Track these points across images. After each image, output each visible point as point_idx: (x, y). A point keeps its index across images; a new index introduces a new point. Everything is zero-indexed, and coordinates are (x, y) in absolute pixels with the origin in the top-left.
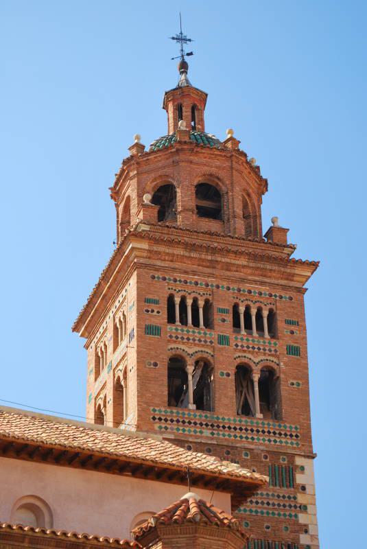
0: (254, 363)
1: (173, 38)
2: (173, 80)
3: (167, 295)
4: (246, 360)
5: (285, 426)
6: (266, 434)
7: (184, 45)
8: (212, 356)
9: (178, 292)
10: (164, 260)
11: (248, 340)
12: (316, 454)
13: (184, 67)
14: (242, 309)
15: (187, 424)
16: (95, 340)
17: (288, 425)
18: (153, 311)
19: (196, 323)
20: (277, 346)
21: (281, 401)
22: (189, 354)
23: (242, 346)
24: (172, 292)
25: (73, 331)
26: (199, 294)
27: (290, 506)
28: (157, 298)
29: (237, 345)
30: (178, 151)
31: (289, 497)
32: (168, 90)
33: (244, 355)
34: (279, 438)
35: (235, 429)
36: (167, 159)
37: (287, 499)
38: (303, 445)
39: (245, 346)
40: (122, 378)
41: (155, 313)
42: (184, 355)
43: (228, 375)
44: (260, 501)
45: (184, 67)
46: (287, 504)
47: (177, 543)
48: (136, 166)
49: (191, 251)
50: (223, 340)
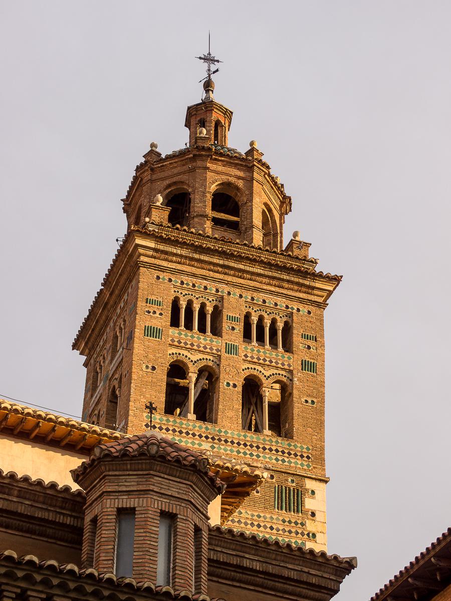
0: (265, 376)
1: (200, 58)
2: (197, 96)
3: (172, 298)
4: (255, 373)
5: (295, 446)
6: (274, 452)
7: (212, 65)
8: (218, 365)
9: (184, 296)
10: (171, 261)
11: (259, 351)
12: (329, 478)
13: (208, 86)
14: (254, 319)
15: (184, 435)
16: (95, 356)
17: (299, 445)
18: (155, 312)
19: (202, 329)
20: (292, 360)
21: (293, 419)
22: (192, 361)
23: (252, 357)
24: (178, 295)
25: (73, 349)
26: (208, 299)
27: (297, 533)
28: (160, 299)
29: (246, 356)
30: (195, 156)
31: (296, 523)
32: (190, 105)
33: (253, 366)
34: (288, 458)
35: (239, 444)
36: (184, 165)
37: (293, 524)
38: (314, 468)
39: (256, 357)
40: (117, 386)
41: (157, 315)
42: (186, 361)
43: (235, 386)
44: (262, 524)
45: (208, 86)
46: (293, 530)
47: (126, 481)
48: (150, 172)
49: (200, 253)
50: (231, 349)
